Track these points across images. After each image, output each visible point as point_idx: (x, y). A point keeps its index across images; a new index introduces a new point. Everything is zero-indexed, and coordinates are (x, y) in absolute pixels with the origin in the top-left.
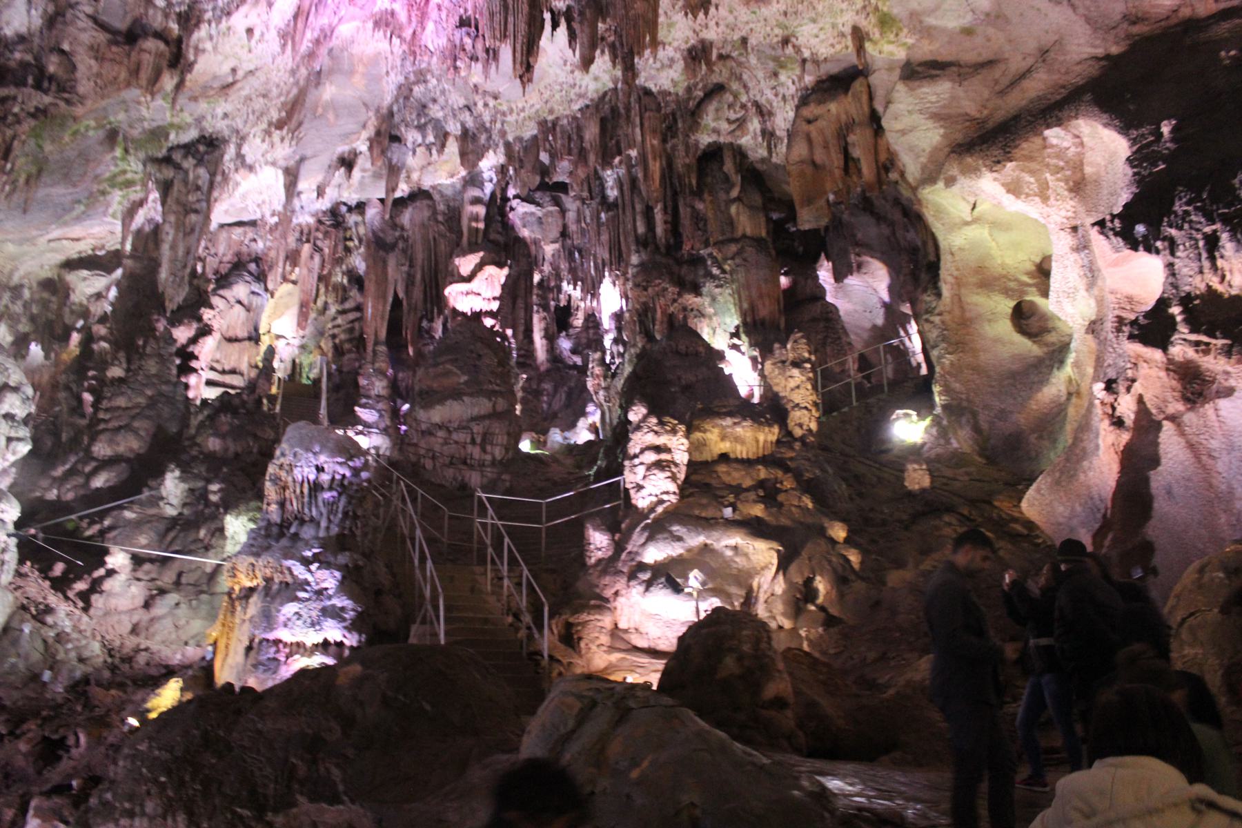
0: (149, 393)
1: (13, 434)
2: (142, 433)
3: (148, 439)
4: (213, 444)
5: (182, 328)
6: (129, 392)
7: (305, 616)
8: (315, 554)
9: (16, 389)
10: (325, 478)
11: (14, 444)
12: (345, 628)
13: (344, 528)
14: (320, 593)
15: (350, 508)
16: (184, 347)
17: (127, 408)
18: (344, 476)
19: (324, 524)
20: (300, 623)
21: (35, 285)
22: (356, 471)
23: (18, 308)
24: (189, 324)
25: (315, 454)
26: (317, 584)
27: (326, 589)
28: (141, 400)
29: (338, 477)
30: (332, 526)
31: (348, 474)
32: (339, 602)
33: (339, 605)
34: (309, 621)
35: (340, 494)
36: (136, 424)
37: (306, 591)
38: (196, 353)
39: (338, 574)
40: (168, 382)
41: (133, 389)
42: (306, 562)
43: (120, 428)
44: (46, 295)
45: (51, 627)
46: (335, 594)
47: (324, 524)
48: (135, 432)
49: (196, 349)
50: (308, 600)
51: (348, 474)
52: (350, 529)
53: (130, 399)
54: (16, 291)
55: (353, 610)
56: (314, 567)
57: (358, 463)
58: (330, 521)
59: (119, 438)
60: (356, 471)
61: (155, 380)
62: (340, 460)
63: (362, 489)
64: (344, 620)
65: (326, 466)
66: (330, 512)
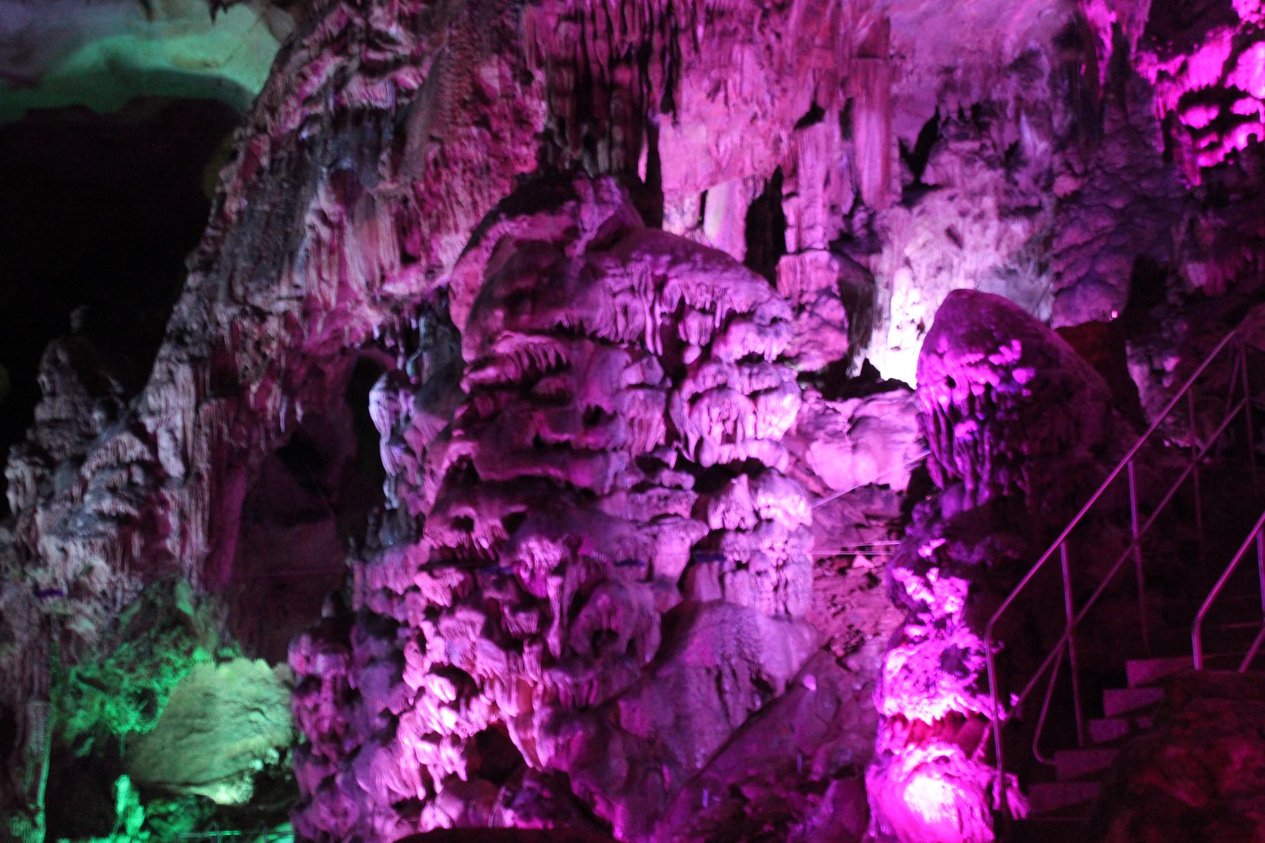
0: (1118, 204)
1: (757, 386)
2: (1112, 281)
3: (1123, 288)
4: (1196, 274)
5: (1206, 50)
6: (1082, 214)
7: (918, 671)
8: (935, 551)
9: (747, 316)
10: (960, 397)
11: (762, 399)
12: (967, 689)
13: (1001, 487)
14: (942, 623)
15: (1002, 446)
16: (1222, 80)
17: (1086, 244)
18: (988, 386)
19: (969, 486)
20: (907, 685)
21: (1049, 46)
22: (1005, 372)
23: (1041, 90)
24: (1217, 38)
25: (941, 356)
26: (939, 606)
27: (950, 615)
28: (1105, 222)
29: (978, 391)
30: (981, 486)
31: (994, 381)
32: (963, 639)
33: (961, 646)
34: (923, 679)
35: (981, 424)
36: (1101, 268)
37: (921, 623)
38: (1241, 86)
39: (962, 585)
40: (1151, 173)
41: (1088, 208)
42: (920, 568)
43: (1080, 280)
44: (1068, 55)
45: (857, 674)
46: (960, 621)
47: (969, 486)
48: (1099, 281)
49: (1238, 79)
50: (924, 638)
51: (994, 381)
52: (1013, 485)
53: (1085, 227)
54: (1025, 63)
55: (978, 653)
56: (932, 576)
57: (1010, 354)
58: (976, 477)
59: (1078, 301)
60: (1005, 372)
61: (1125, 177)
62: (972, 358)
63: (1021, 404)
64: (965, 673)
65: (954, 376)
66: (976, 460)
